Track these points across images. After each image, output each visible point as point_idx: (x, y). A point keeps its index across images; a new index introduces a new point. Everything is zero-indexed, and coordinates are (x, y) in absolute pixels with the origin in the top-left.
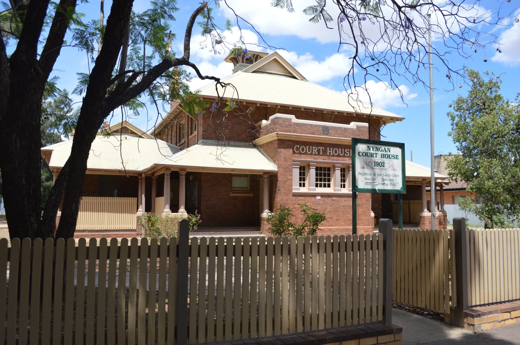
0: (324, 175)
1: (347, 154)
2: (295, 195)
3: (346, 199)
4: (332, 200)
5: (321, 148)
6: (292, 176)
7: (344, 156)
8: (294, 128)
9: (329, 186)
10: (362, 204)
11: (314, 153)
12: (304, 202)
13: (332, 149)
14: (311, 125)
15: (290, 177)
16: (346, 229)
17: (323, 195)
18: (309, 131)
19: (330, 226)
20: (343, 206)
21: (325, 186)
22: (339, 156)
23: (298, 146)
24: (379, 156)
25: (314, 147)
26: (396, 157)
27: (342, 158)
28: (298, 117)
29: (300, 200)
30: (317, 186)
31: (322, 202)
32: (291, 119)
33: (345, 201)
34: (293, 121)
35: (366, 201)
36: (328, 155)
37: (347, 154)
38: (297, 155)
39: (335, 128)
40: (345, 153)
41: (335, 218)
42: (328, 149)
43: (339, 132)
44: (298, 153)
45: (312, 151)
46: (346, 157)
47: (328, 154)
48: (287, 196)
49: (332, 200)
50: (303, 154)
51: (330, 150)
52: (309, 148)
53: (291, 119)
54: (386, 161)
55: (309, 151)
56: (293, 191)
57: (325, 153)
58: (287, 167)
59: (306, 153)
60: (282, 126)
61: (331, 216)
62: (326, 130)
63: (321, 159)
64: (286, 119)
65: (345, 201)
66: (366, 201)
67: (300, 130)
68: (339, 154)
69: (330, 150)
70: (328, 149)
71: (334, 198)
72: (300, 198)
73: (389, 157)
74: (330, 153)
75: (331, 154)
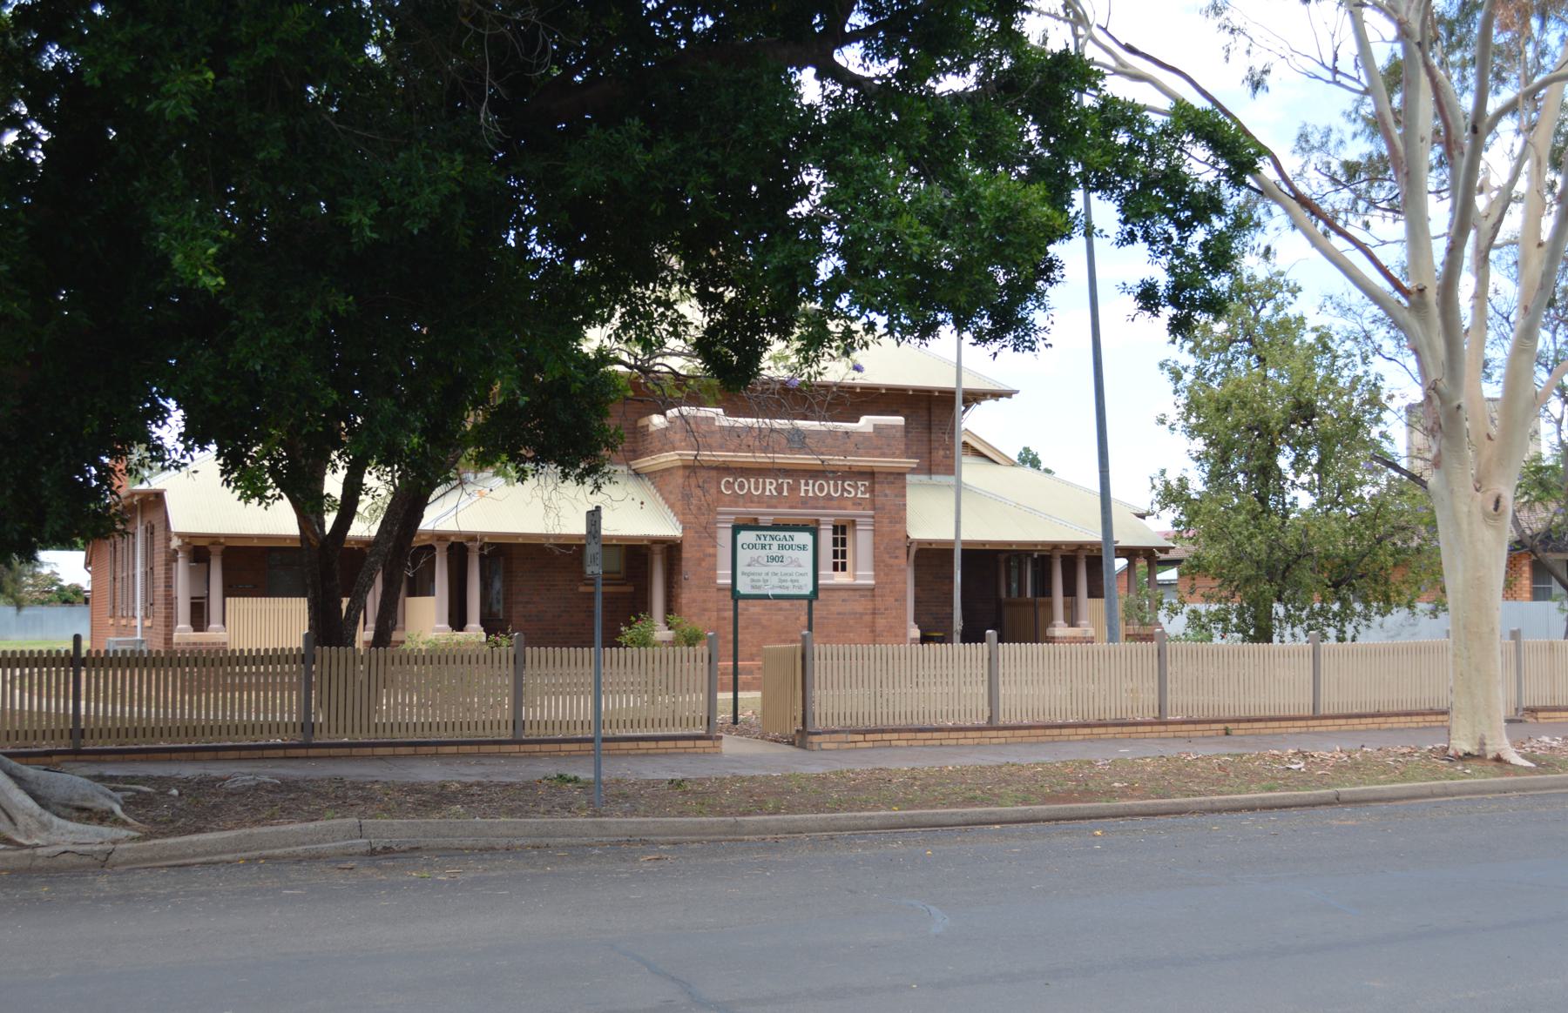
15: (711, 550)
24: (775, 547)
26: (804, 548)
28: (730, 412)
40: (844, 489)
51: (807, 484)
52: (757, 483)
54: (784, 552)
55: (757, 489)
69: (807, 484)
73: (791, 547)
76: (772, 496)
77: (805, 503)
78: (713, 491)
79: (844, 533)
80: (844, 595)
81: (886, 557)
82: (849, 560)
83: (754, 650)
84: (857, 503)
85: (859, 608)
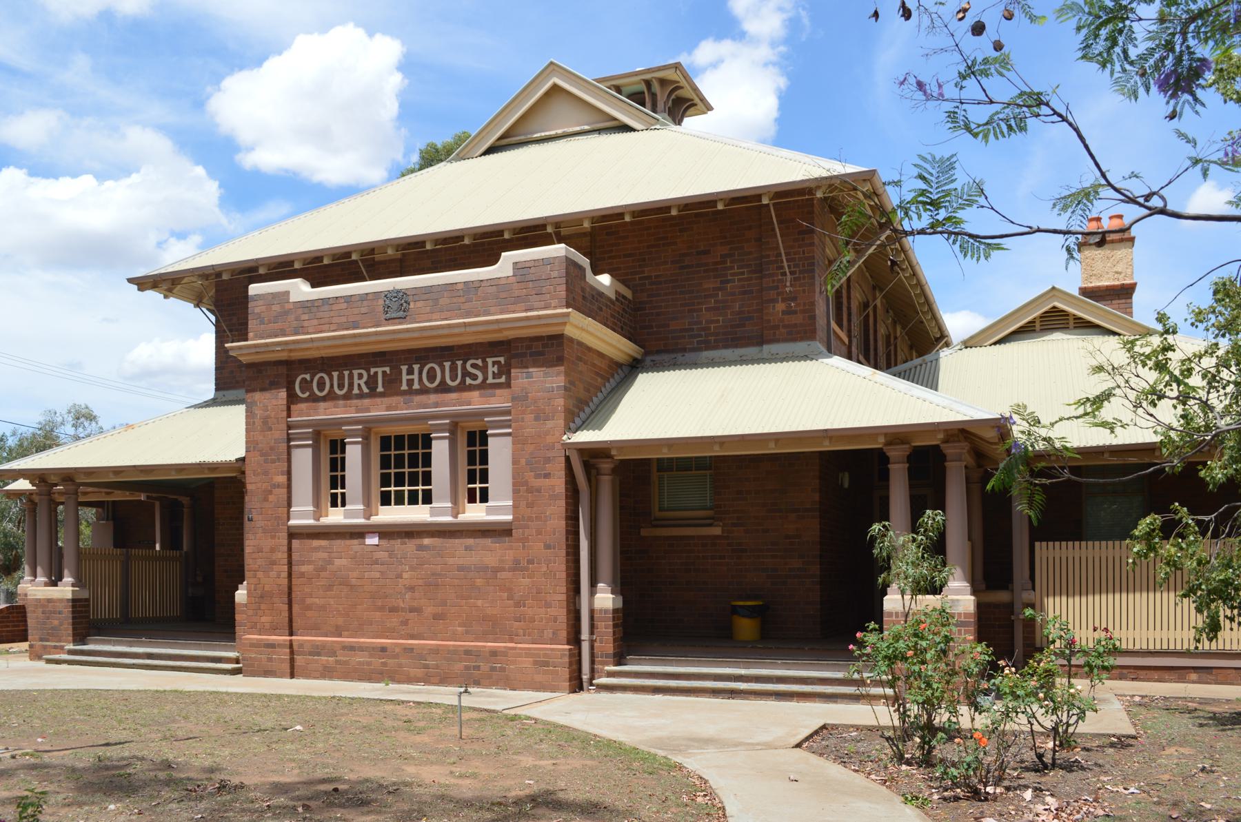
0: (402, 466)
1: (475, 377)
2: (293, 534)
3: (470, 541)
4: (421, 548)
5: (380, 370)
7: (463, 388)
8: (297, 319)
9: (428, 499)
10: (530, 562)
11: (356, 391)
12: (325, 555)
13: (416, 367)
14: (348, 299)
16: (468, 652)
17: (389, 532)
18: (344, 319)
19: (413, 637)
20: (461, 568)
21: (413, 500)
22: (443, 388)
23: (308, 377)
25: (356, 372)
27: (454, 396)
29: (317, 549)
30: (386, 500)
31: (382, 555)
32: (287, 293)
33: (467, 548)
34: (294, 298)
35: (547, 547)
36: (404, 393)
37: (475, 377)
38: (303, 406)
39: (428, 290)
40: (466, 374)
41: (429, 610)
42: (404, 368)
43: (444, 301)
44: (306, 400)
45: (351, 385)
46: (471, 388)
47: (404, 387)
48: (273, 537)
49: (421, 548)
50: (324, 399)
51: (410, 372)
52: (341, 378)
53: (287, 293)
55: (341, 386)
56: (292, 522)
57: (392, 384)
58: (272, 449)
59: (331, 397)
60: (262, 323)
61: (415, 604)
62: (399, 304)
63: (378, 409)
64: (275, 295)
65: (467, 548)
66: (547, 547)
67: (315, 322)
68: (443, 382)
69: (410, 372)
70: (404, 368)
71: (427, 541)
72: (316, 543)
74: (410, 382)
75: (416, 386)
79: (484, 442)
81: (529, 476)
83: (340, 621)
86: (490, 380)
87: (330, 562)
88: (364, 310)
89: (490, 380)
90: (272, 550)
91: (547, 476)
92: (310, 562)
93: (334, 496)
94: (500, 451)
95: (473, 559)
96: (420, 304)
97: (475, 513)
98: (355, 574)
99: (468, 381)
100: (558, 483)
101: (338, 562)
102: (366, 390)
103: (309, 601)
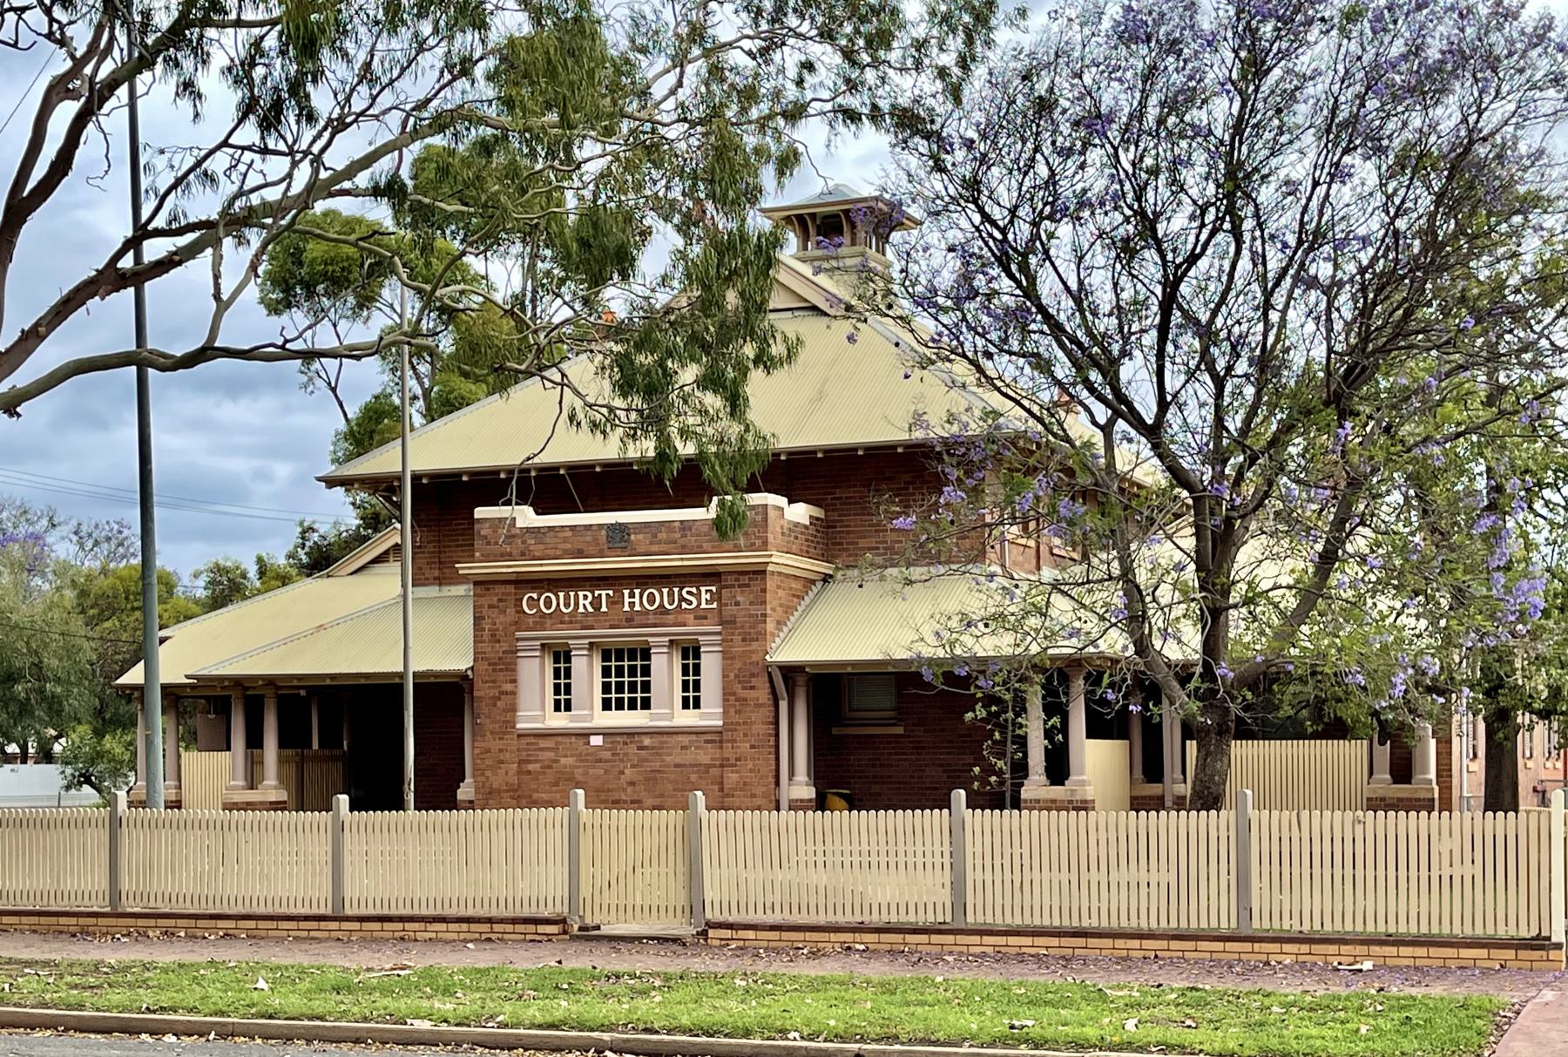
5: (604, 593)
6: (514, 681)
9: (646, 704)
12: (551, 755)
13: (637, 592)
14: (572, 528)
15: (508, 687)
20: (676, 766)
21: (633, 706)
23: (535, 596)
25: (581, 594)
30: (606, 705)
31: (608, 755)
40: (682, 599)
42: (626, 592)
43: (663, 536)
45: (577, 604)
51: (632, 595)
52: (567, 598)
55: (567, 605)
60: (488, 543)
62: (619, 537)
66: (752, 747)
68: (661, 605)
69: (632, 595)
70: (626, 592)
75: (637, 608)
76: (586, 614)
77: (630, 620)
78: (511, 611)
80: (685, 740)
81: (738, 688)
82: (654, 695)
84: (701, 616)
85: (704, 758)
86: (704, 606)
87: (557, 761)
88: (588, 539)
89: (704, 606)
90: (501, 751)
91: (752, 688)
92: (537, 761)
93: (557, 703)
94: (711, 664)
95: (687, 758)
96: (640, 537)
97: (689, 718)
98: (580, 771)
99: (684, 605)
100: (763, 694)
101: (563, 761)
102: (590, 609)
103: (535, 796)
